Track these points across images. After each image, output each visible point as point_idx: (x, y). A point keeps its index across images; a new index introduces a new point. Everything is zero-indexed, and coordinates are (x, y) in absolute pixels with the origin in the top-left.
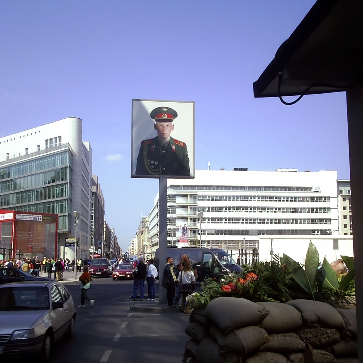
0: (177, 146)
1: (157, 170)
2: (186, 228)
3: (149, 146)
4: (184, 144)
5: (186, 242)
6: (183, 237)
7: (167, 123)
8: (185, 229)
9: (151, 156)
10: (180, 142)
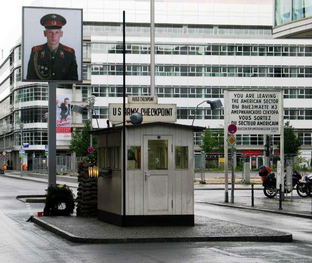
0: (65, 52)
1: (47, 75)
2: (69, 105)
3: (40, 54)
4: (73, 51)
5: (68, 132)
6: (63, 123)
7: (56, 30)
8: (66, 107)
9: (41, 62)
10: (68, 48)
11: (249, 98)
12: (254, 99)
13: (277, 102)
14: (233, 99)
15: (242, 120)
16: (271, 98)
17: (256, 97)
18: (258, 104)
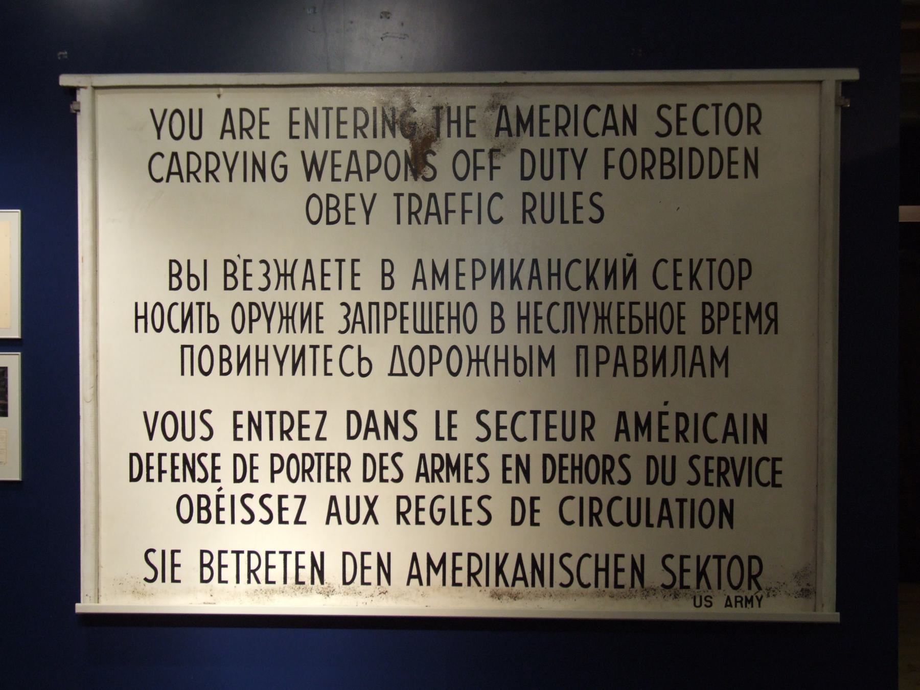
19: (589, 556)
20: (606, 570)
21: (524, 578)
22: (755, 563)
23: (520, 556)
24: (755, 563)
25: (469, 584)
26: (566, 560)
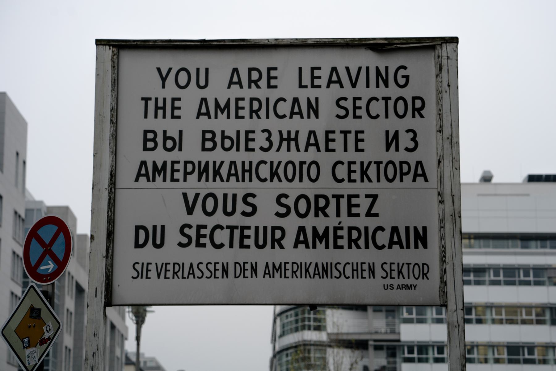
11: (248, 93)
12: (274, 95)
13: (418, 111)
14: (146, 100)
15: (198, 217)
16: (382, 92)
17: (287, 87)
18: (302, 126)
19: (349, 263)
20: (357, 270)
21: (319, 274)
22: (425, 266)
23: (317, 264)
24: (425, 266)
25: (292, 277)
26: (338, 266)
